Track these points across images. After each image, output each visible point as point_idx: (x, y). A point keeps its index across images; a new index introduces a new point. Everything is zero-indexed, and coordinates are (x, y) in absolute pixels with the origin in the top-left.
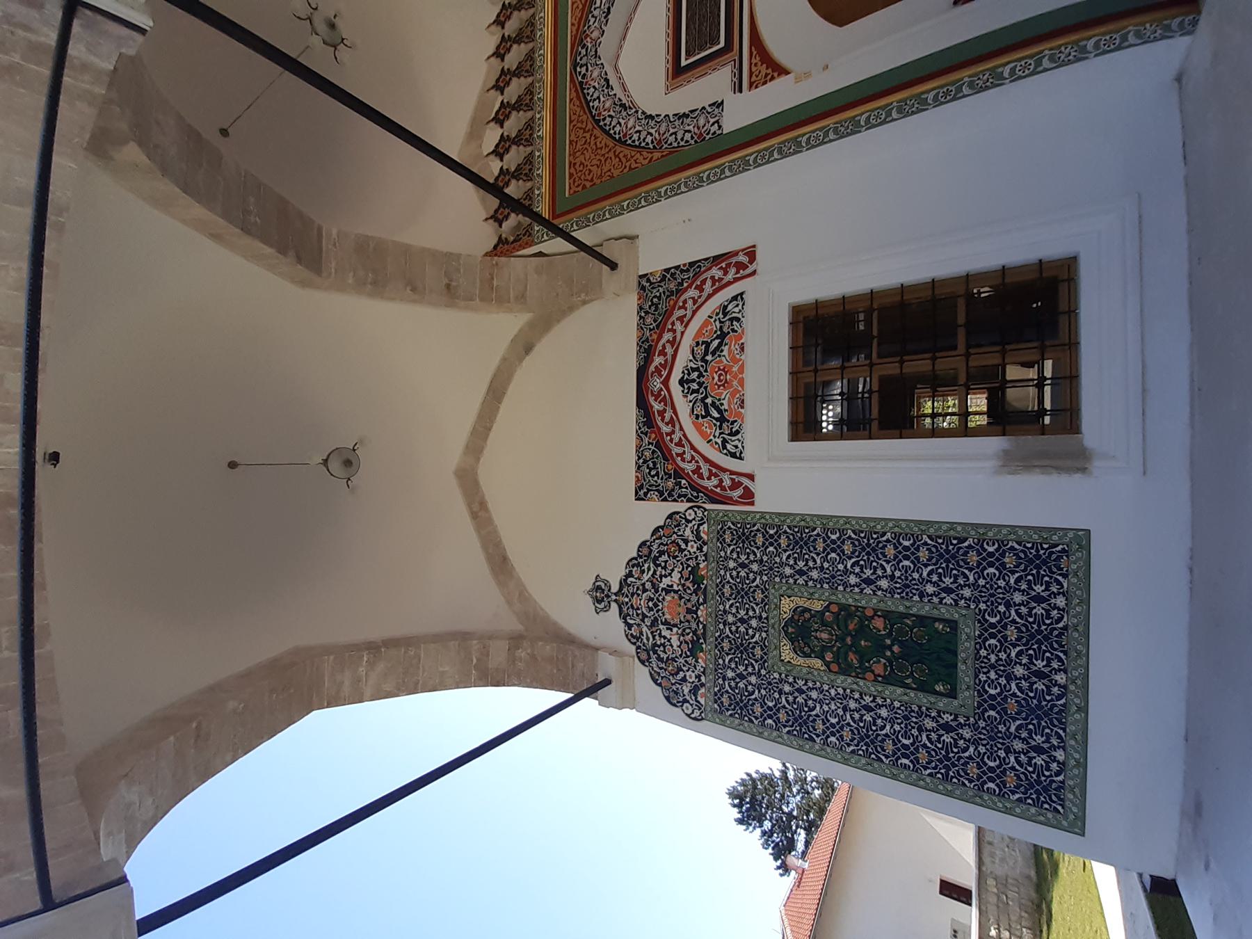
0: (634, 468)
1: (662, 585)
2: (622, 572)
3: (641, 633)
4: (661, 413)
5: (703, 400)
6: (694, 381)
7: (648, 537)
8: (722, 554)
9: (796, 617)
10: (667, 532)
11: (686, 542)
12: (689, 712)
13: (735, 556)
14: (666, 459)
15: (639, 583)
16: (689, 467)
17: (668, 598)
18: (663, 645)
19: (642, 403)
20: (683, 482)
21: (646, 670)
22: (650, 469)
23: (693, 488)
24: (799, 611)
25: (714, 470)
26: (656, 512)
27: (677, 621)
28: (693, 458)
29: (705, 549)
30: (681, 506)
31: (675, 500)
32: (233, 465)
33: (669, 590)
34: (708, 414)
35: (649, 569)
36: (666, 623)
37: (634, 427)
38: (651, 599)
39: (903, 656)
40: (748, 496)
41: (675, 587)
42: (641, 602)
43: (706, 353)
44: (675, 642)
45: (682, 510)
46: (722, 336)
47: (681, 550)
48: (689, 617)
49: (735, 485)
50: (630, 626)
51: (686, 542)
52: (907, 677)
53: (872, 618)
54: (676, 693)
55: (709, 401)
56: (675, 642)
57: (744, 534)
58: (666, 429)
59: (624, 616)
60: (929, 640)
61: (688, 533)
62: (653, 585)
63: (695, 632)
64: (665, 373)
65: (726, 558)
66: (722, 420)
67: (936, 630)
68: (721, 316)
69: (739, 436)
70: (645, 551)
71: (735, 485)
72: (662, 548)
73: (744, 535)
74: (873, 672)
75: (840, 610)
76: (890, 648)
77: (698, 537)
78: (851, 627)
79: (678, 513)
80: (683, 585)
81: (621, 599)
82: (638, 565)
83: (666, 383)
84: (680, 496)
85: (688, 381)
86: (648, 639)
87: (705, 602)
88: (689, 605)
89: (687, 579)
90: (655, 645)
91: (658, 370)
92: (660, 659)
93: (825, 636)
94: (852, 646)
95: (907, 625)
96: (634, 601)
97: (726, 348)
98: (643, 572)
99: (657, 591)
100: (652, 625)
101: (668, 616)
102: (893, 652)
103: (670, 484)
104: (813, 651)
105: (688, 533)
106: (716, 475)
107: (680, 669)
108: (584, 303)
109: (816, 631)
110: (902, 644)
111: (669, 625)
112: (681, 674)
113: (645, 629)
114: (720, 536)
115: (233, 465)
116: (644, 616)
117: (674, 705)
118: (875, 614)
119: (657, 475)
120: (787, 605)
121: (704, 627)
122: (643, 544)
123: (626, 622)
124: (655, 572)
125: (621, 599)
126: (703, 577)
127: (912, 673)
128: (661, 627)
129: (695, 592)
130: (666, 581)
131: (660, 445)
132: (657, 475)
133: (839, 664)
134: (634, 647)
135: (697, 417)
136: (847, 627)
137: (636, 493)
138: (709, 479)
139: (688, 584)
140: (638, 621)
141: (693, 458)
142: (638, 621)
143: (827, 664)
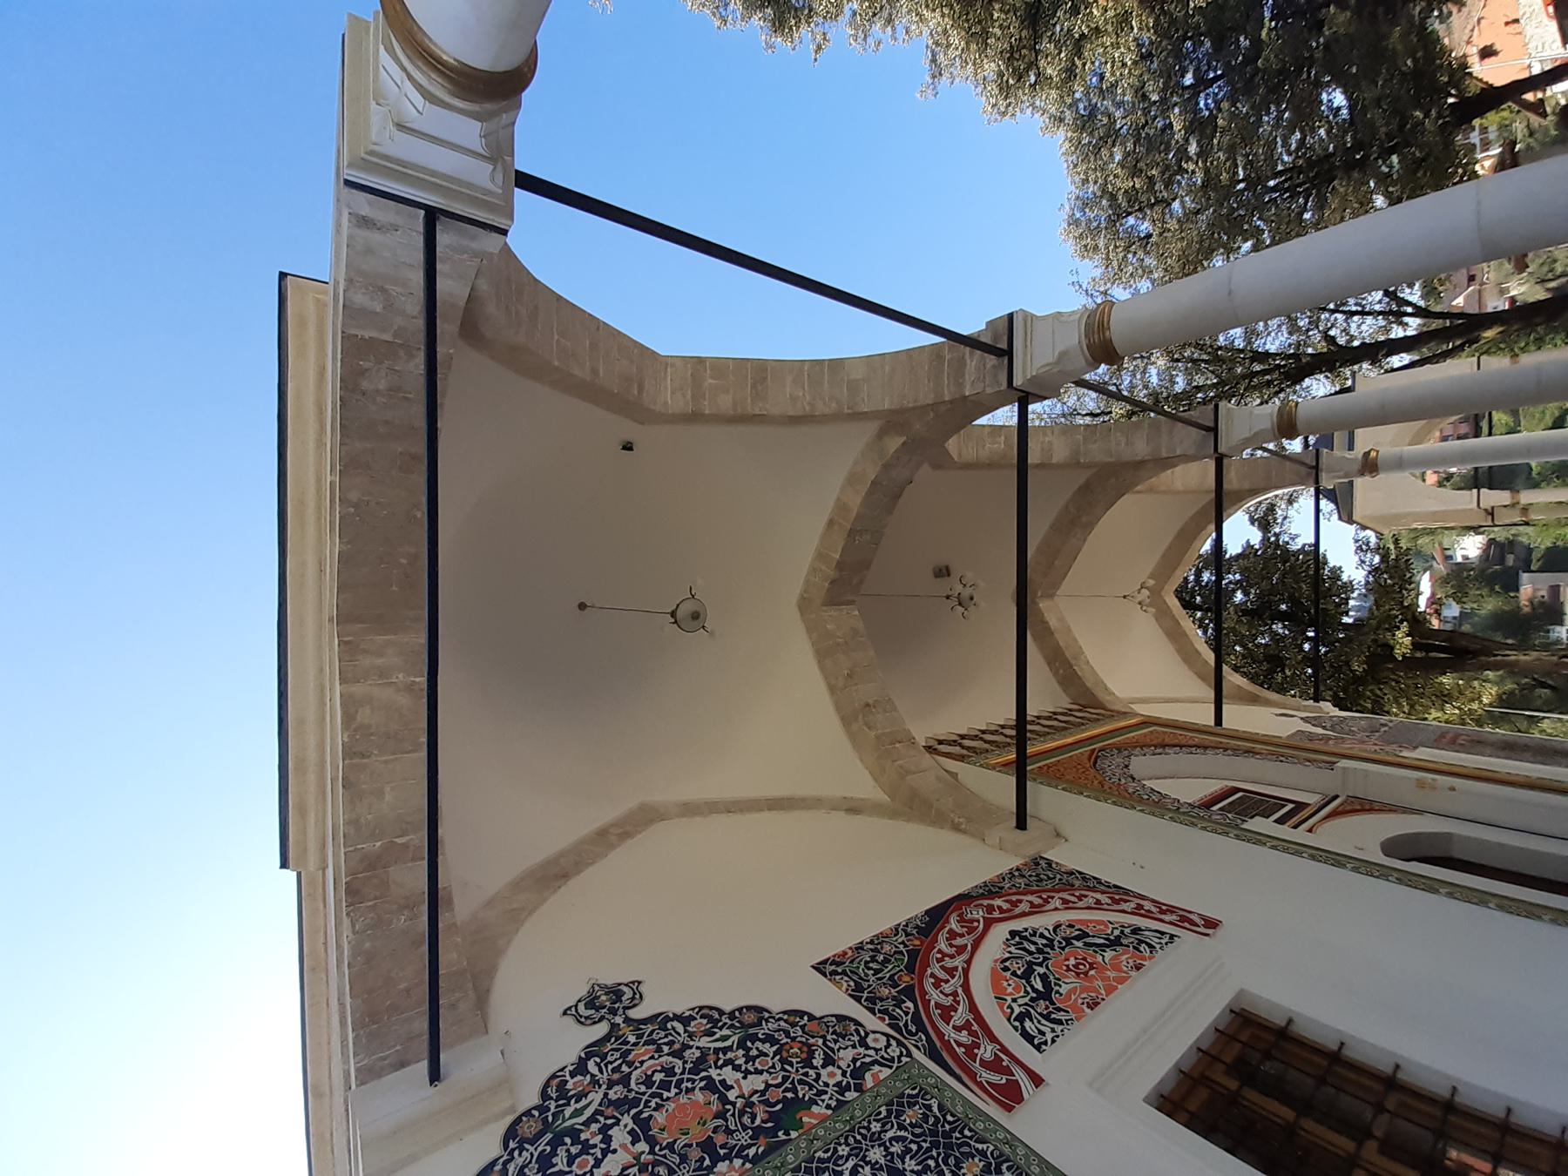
0: (854, 942)
1: (713, 1073)
4: (953, 935)
5: (1030, 964)
6: (1035, 943)
8: (875, 1127)
11: (829, 1061)
13: (896, 1148)
14: (910, 968)
15: (683, 1038)
16: (935, 996)
17: (699, 1096)
18: (586, 1148)
19: (937, 915)
20: (910, 1005)
21: (493, 1150)
22: (873, 959)
23: (916, 1018)
25: (975, 1027)
26: (830, 999)
27: (665, 1138)
28: (955, 994)
29: (851, 1095)
30: (871, 1021)
31: (872, 1011)
32: (582, 606)
33: (710, 1086)
34: (1027, 975)
37: (901, 919)
38: (669, 1071)
40: (1010, 1096)
41: (731, 1095)
42: (647, 1062)
43: (1078, 938)
45: (869, 1027)
46: (1115, 943)
47: (808, 1063)
48: (695, 1154)
49: (994, 1065)
50: (580, 1068)
55: (1042, 970)
57: (947, 1135)
58: (942, 945)
61: (846, 1056)
64: (996, 915)
65: (876, 1139)
66: (1046, 995)
68: (1127, 931)
69: (1058, 1028)
70: (749, 1018)
71: (994, 1065)
73: (947, 1136)
77: (858, 1072)
82: (714, 1022)
83: (989, 923)
84: (885, 1012)
85: (1025, 938)
87: (755, 1160)
88: (720, 1139)
89: (767, 1103)
90: (574, 1133)
91: (990, 909)
97: (1109, 954)
98: (709, 1033)
99: (695, 1070)
100: (617, 1104)
101: (660, 1117)
103: (885, 992)
105: (846, 1056)
106: (972, 1033)
108: (956, 828)
111: (643, 1129)
113: (596, 1097)
114: (897, 1106)
115: (582, 606)
116: (625, 1081)
119: (877, 972)
122: (759, 1009)
124: (730, 1048)
126: (799, 1125)
129: (757, 1133)
130: (729, 1074)
131: (916, 961)
132: (877, 972)
135: (1006, 969)
137: (824, 962)
138: (958, 1029)
141: (955, 994)
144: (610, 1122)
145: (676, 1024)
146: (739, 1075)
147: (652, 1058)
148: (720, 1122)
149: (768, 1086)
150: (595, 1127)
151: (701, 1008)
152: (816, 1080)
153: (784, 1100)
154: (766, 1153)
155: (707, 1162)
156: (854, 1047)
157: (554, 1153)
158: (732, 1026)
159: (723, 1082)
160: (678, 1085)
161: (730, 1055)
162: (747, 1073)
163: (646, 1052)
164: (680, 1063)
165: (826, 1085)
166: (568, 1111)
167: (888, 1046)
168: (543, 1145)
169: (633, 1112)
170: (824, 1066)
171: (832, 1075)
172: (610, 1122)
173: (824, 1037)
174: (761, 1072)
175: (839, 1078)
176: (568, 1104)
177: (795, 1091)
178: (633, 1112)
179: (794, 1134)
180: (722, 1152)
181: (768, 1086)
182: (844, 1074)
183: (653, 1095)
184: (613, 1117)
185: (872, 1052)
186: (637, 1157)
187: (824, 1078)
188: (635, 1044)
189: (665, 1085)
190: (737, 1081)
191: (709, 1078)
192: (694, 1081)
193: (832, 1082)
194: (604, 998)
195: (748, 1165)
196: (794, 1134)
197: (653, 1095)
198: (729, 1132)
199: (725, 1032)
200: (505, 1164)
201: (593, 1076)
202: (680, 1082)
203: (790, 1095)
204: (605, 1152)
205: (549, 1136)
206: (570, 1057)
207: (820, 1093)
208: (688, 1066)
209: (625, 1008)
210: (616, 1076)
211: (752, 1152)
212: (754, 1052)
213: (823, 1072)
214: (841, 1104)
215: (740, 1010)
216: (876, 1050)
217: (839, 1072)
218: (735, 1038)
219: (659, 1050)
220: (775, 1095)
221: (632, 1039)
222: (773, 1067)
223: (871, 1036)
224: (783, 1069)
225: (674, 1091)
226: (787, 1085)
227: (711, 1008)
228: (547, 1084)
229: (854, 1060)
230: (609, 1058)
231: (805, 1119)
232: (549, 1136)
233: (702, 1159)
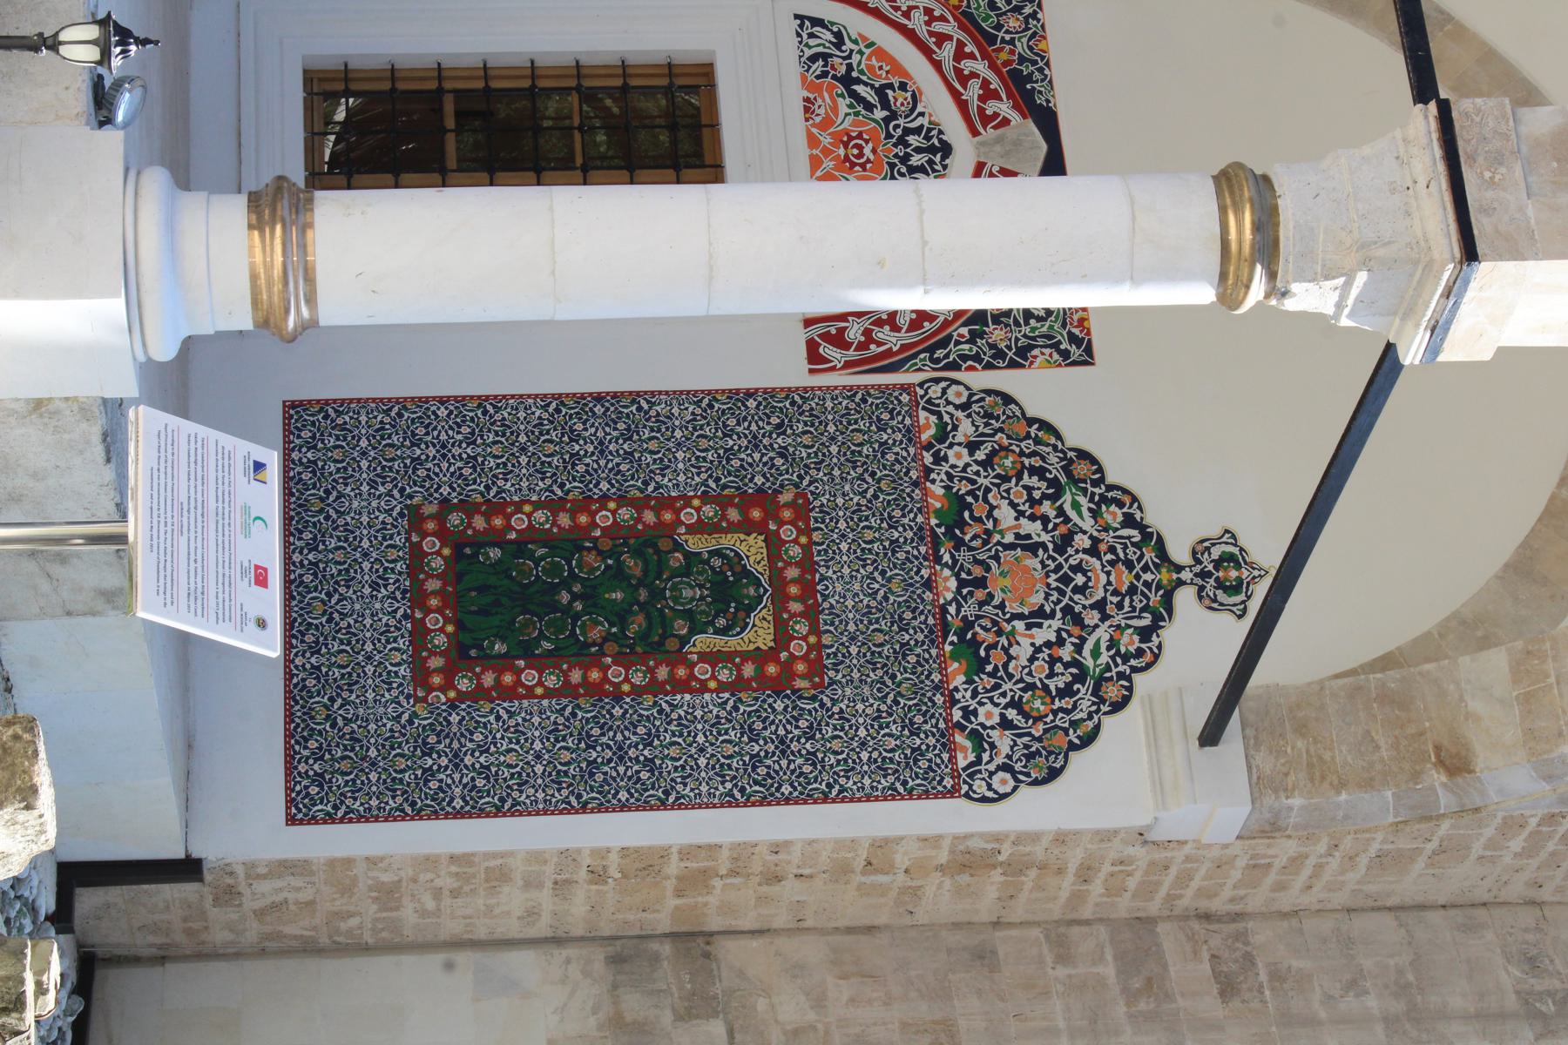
1: (1056, 623)
2: (1169, 635)
3: (1095, 514)
7: (1110, 724)
9: (741, 615)
10: (1059, 741)
12: (954, 387)
15: (1119, 619)
17: (1037, 599)
29: (957, 715)
35: (1096, 653)
36: (1033, 549)
39: (554, 589)
41: (1020, 625)
44: (1006, 515)
47: (1015, 704)
48: (978, 571)
50: (1129, 521)
51: (1005, 724)
52: (542, 558)
53: (605, 640)
54: (988, 415)
56: (1006, 515)
60: (514, 621)
61: (1003, 741)
62: (1078, 620)
63: (959, 544)
67: (503, 639)
70: (1112, 692)
72: (1066, 703)
74: (600, 553)
75: (661, 644)
76: (575, 597)
77: (977, 737)
78: (641, 618)
79: (1036, 783)
80: (1000, 633)
81: (1165, 576)
82: (1126, 658)
86: (1076, 506)
87: (944, 610)
88: (980, 594)
89: (994, 646)
92: (1040, 472)
93: (687, 593)
94: (637, 587)
95: (548, 639)
96: (1127, 578)
98: (1112, 644)
99: (1067, 610)
100: (1067, 539)
101: (1033, 563)
102: (570, 591)
104: (707, 562)
105: (1003, 741)
107: (987, 463)
109: (702, 598)
110: (554, 607)
112: (980, 455)
116: (1093, 551)
117: (989, 392)
118: (601, 646)
121: (938, 559)
122: (1118, 706)
123: (1141, 527)
124: (1079, 648)
125: (1165, 576)
126: (955, 656)
127: (537, 566)
128: (1045, 537)
129: (968, 624)
133: (658, 552)
134: (1111, 479)
136: (648, 617)
139: (990, 638)
140: (1108, 538)
142: (1108, 538)
143: (677, 547)
144: (1050, 526)
145: (1146, 621)
146: (1038, 642)
147: (1109, 583)
148: (996, 602)
149: (1010, 658)
150: (1052, 514)
151: (1156, 657)
152: (991, 699)
153: (987, 661)
154: (943, 619)
155: (964, 575)
156: (1009, 757)
157: (1042, 478)
158: (1108, 669)
159: (1040, 626)
160: (1057, 589)
161: (1069, 648)
162: (1038, 650)
163: (1119, 577)
164: (1087, 603)
165: (981, 704)
166: (1083, 500)
167: (990, 787)
168: (1055, 471)
169: (1051, 546)
170: (1002, 716)
171: (989, 715)
172: (1050, 526)
173: (1039, 739)
174: (1032, 659)
175: (981, 719)
176: (1091, 500)
177: (992, 675)
178: (1051, 546)
179: (948, 648)
180: (965, 591)
181: (1010, 658)
182: (981, 724)
183: (1059, 567)
184: (1054, 529)
185: (992, 767)
186: (1002, 533)
187: (989, 706)
188: (1138, 577)
189: (1065, 580)
190: (1032, 636)
191: (1052, 615)
192: (1056, 604)
193: (981, 710)
194: (1234, 574)
195: (942, 601)
196: (948, 648)
197: (1059, 567)
198: (981, 604)
199: (1104, 658)
200: (1055, 448)
201: (1116, 530)
202: (1062, 593)
203: (989, 668)
204: (1021, 514)
205: (1063, 479)
206: (1154, 518)
207: (975, 694)
208: (1077, 609)
209: (1201, 588)
210: (1103, 547)
211: (952, 609)
212: (1059, 668)
213: (996, 711)
214: (954, 702)
215: (1130, 689)
216: (991, 774)
217: (988, 724)
218: (1089, 663)
219: (1116, 593)
220: (997, 658)
221: (1148, 577)
222: (1030, 674)
223: (1012, 783)
224: (1021, 680)
225: (1054, 584)
226: (1001, 673)
227: (1149, 666)
228: (1125, 491)
229: (993, 746)
230: (1131, 549)
231: (956, 665)
232: (1063, 479)
233: (969, 573)
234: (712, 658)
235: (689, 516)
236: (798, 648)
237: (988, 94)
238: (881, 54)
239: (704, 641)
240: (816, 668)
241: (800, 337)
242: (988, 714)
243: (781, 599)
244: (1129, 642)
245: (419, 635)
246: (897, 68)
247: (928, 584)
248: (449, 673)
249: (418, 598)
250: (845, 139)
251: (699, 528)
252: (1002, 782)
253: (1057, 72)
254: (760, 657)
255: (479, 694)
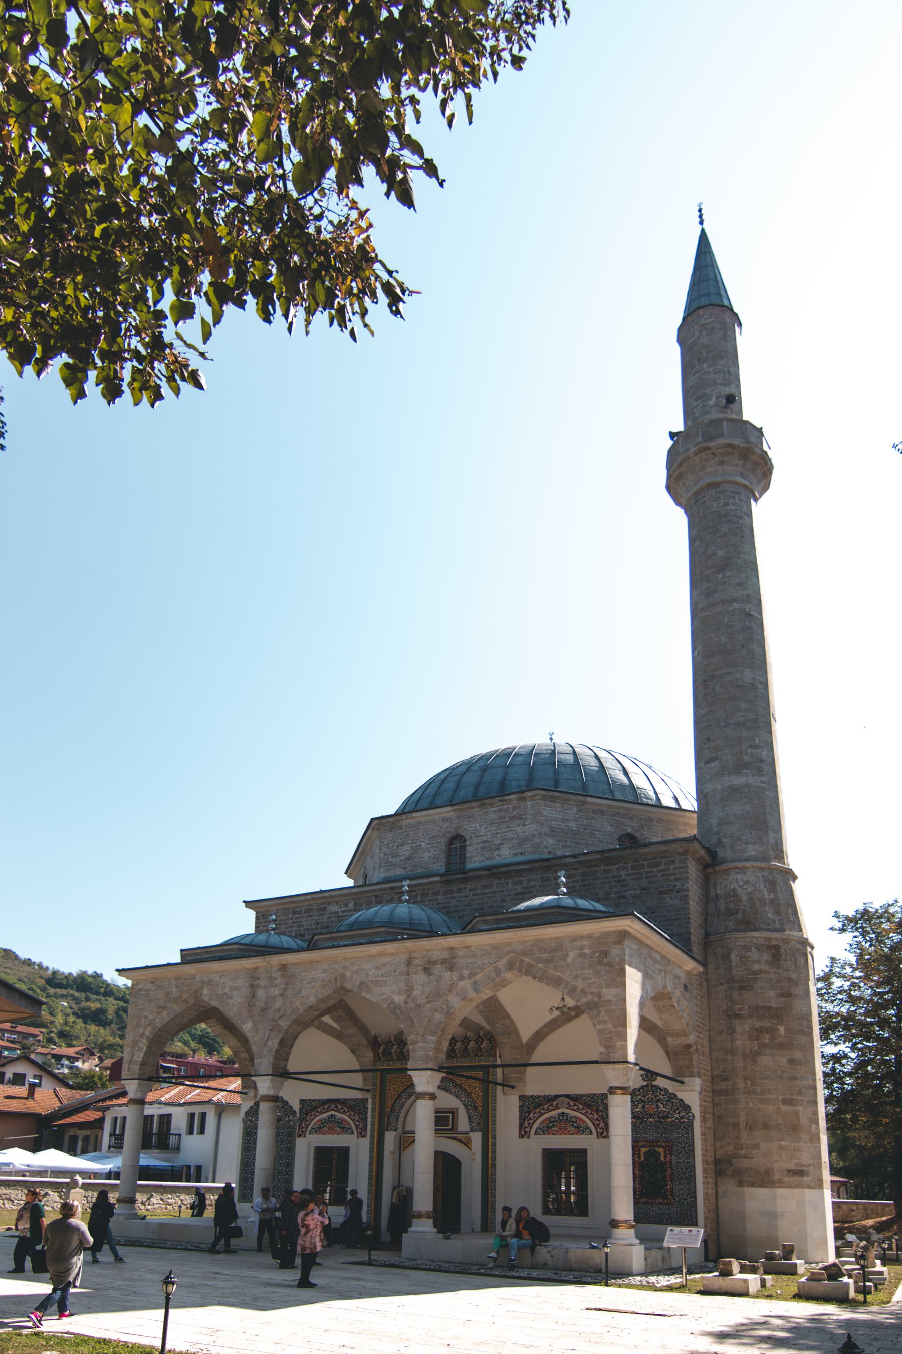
24: (659, 1154)
33: (658, 1107)
50: (639, 1090)
59: (643, 1087)
105: (682, 1114)
111: (643, 1107)
120: (661, 1150)
130: (661, 1106)
206: (638, 1086)
234: (665, 1157)
235: (637, 1159)
236: (663, 1144)
237: (552, 1105)
238: (543, 1122)
239: (662, 1159)
240: (668, 1142)
241: (601, 1140)
242: (677, 1116)
243: (654, 1146)
244: (663, 1093)
245: (660, 1203)
246: (546, 1119)
247: (651, 1123)
248: (668, 1199)
249: (653, 1203)
250: (560, 1129)
251: (639, 1158)
252: (690, 1115)
253: (547, 1093)
254: (665, 1151)
255: (672, 1195)
